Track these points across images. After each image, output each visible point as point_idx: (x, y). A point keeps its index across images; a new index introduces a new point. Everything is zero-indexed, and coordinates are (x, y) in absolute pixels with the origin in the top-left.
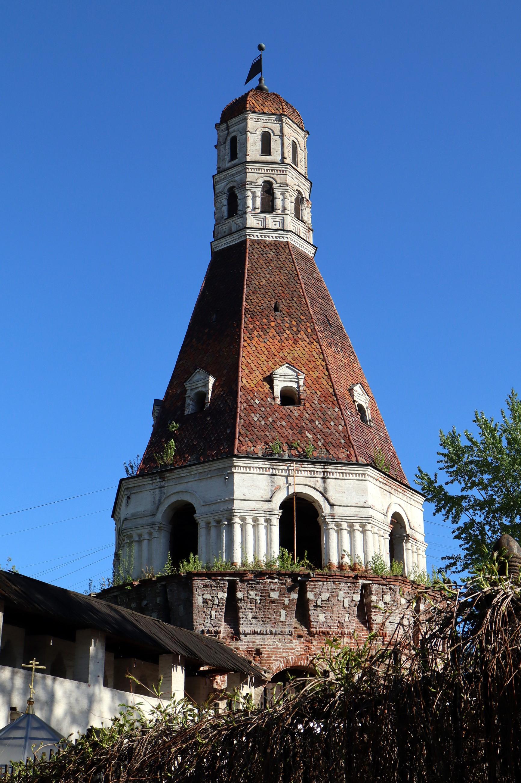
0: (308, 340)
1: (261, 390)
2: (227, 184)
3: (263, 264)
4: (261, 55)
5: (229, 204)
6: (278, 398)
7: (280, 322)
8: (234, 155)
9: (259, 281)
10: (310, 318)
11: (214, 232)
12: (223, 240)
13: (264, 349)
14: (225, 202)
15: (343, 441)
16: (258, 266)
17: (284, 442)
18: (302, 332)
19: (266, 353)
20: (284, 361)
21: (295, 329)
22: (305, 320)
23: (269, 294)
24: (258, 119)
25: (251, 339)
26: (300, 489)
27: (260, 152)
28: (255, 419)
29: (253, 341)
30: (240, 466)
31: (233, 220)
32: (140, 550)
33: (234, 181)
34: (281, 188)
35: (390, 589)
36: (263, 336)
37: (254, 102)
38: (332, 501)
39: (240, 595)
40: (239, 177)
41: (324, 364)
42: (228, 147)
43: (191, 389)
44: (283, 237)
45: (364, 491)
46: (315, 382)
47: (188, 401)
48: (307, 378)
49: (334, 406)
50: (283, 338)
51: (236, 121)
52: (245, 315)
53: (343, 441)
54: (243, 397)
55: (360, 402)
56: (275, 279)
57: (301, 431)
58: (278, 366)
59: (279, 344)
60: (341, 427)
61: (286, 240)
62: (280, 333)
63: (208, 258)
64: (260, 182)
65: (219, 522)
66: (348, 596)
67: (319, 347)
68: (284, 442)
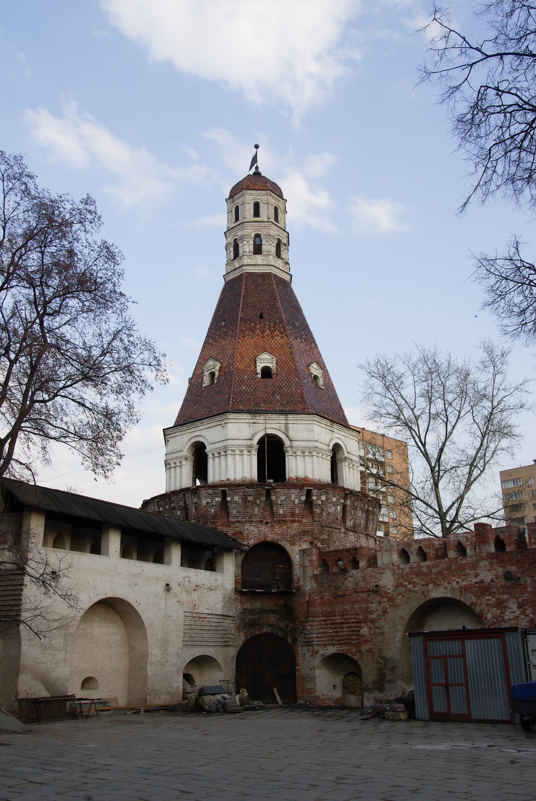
0: (281, 336)
1: (248, 369)
8: (237, 219)
10: (282, 321)
13: (251, 343)
14: (232, 249)
15: (300, 400)
17: (261, 402)
18: (277, 331)
19: (253, 345)
21: (272, 329)
25: (244, 337)
26: (269, 431)
27: (253, 215)
28: (244, 388)
29: (245, 339)
32: (175, 473)
35: (325, 492)
36: (251, 335)
38: (291, 438)
39: (229, 499)
41: (290, 350)
42: (234, 213)
45: (312, 431)
46: (284, 363)
47: (205, 378)
48: (279, 361)
49: (295, 377)
50: (264, 335)
53: (300, 400)
54: (237, 374)
55: (315, 374)
57: (273, 394)
59: (261, 339)
60: (299, 391)
61: (270, 271)
62: (263, 332)
64: (253, 235)
65: (219, 453)
66: (297, 497)
68: (261, 402)
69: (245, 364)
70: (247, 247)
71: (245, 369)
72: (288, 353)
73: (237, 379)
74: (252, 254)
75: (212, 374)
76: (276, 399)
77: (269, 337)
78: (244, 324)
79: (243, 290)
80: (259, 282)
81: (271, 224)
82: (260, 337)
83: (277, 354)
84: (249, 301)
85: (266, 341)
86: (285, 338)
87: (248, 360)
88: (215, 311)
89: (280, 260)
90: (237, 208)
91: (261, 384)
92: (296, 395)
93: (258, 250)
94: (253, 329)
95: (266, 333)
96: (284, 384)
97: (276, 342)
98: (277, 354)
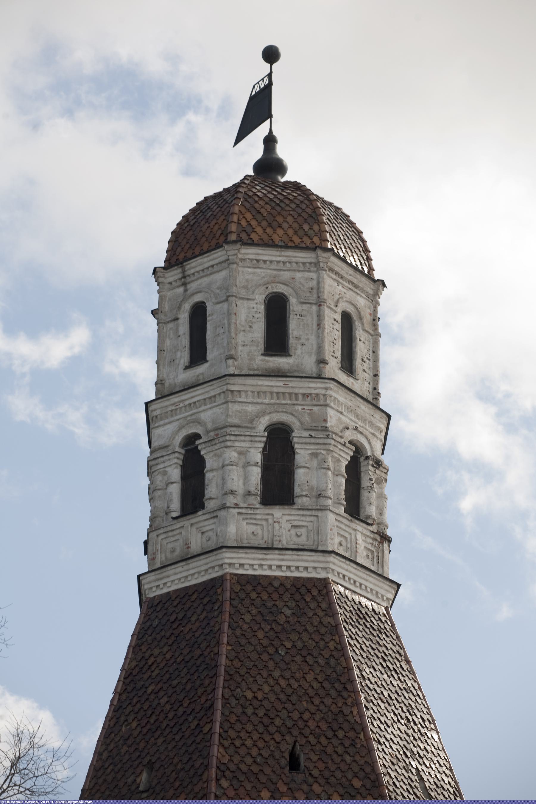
2: (181, 428)
3: (265, 642)
4: (270, 75)
5: (184, 477)
8: (198, 354)
9: (255, 687)
12: (170, 571)
14: (175, 474)
16: (251, 648)
22: (363, 790)
23: (278, 722)
24: (258, 261)
27: (261, 347)
31: (193, 521)
33: (198, 422)
34: (313, 440)
37: (248, 216)
40: (209, 413)
44: (315, 568)
51: (206, 265)
52: (218, 780)
56: (292, 681)
61: (322, 575)
70: (238, 470)
74: (255, 501)
79: (224, 649)
80: (282, 619)
81: (332, 385)
84: (249, 695)
88: (109, 719)
89: (360, 527)
90: (199, 313)
93: (278, 487)
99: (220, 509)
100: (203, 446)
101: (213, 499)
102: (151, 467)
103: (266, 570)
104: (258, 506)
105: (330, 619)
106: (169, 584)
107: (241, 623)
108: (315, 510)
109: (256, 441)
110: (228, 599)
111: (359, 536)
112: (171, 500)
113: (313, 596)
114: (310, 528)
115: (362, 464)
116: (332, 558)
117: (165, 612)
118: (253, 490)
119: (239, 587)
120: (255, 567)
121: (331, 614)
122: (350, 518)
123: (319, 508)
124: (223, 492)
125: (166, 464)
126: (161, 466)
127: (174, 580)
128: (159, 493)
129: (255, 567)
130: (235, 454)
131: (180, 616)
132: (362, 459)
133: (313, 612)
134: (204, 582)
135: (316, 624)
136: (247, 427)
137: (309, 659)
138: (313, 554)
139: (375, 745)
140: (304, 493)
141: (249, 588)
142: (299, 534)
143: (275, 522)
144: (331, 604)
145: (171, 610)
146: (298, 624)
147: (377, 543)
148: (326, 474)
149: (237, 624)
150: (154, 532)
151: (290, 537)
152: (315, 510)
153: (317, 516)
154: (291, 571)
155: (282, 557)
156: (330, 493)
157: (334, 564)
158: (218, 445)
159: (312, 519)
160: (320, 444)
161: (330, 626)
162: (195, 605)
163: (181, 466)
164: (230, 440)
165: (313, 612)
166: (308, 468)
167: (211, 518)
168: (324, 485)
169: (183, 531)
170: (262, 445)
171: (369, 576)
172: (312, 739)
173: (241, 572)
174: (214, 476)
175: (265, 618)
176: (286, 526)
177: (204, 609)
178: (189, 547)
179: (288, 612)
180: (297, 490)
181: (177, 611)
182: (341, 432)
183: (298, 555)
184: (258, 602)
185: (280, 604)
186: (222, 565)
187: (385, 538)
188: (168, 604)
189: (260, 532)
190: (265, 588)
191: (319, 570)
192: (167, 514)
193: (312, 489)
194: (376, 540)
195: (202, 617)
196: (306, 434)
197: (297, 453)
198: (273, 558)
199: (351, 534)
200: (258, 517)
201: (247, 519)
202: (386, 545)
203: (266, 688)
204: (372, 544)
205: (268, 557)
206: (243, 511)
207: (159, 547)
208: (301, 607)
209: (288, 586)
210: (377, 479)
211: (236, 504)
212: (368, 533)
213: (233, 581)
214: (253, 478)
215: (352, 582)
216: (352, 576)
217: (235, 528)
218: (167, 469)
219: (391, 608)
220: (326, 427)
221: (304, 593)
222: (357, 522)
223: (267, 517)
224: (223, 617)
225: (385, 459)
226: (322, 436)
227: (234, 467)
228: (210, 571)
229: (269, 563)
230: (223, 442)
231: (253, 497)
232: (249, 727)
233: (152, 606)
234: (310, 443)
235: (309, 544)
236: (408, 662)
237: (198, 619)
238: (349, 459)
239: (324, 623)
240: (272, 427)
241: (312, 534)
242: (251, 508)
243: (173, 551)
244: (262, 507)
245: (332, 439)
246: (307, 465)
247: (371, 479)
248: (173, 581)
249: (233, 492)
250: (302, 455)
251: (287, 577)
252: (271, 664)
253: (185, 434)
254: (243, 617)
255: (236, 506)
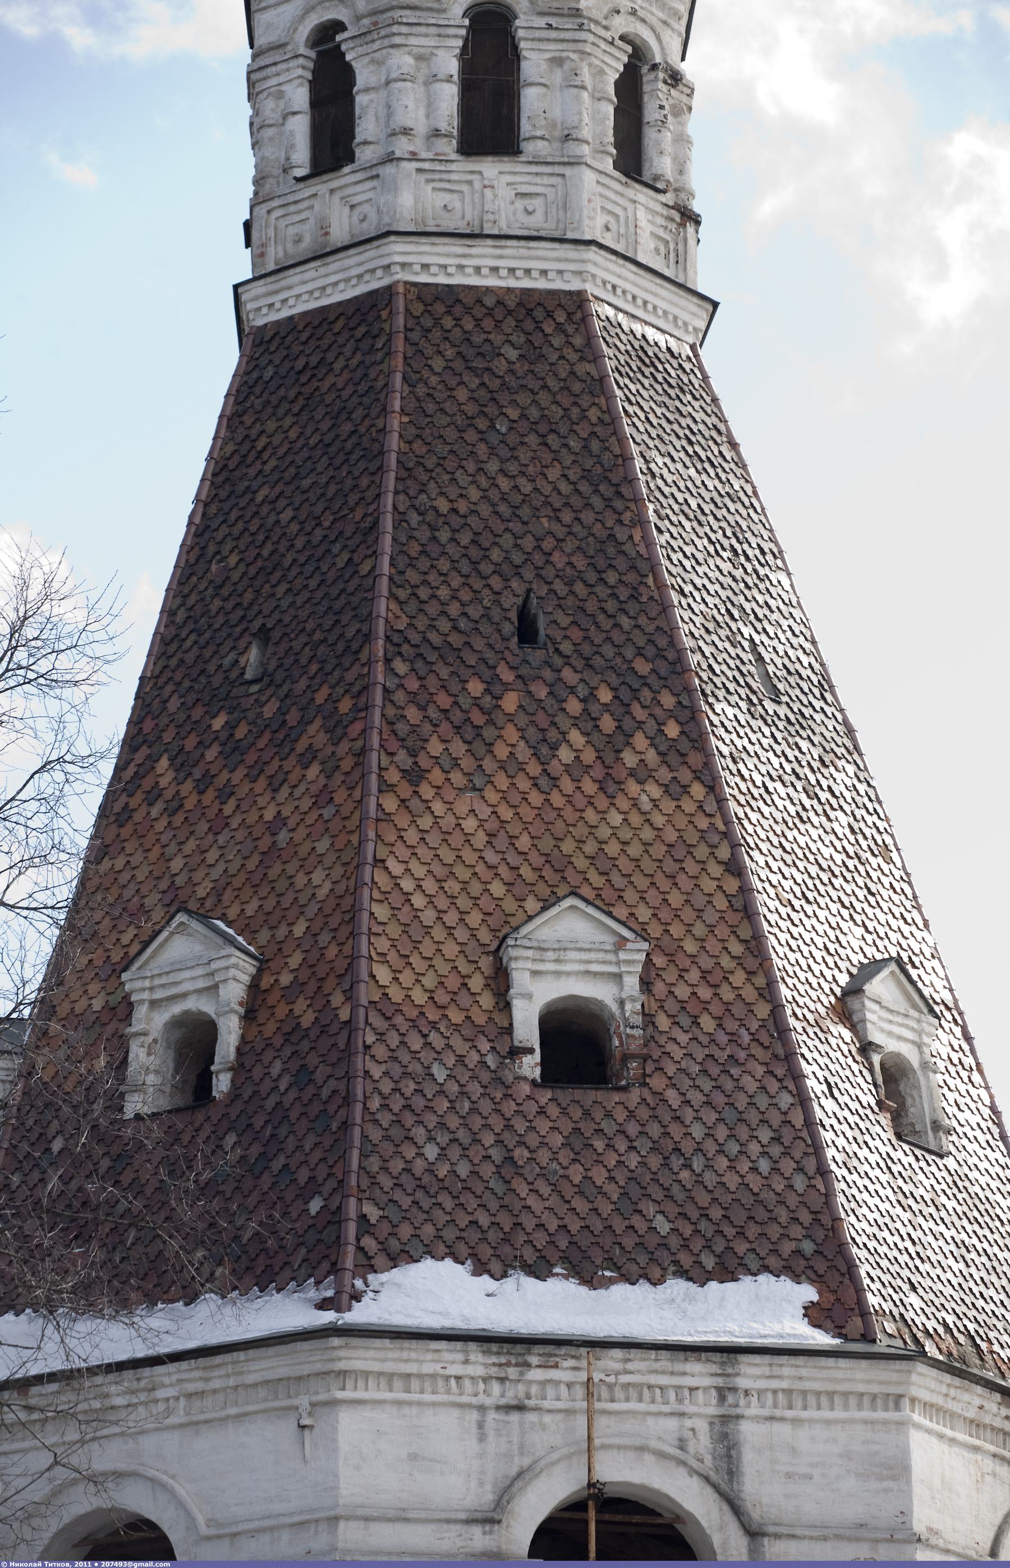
0: (664, 774)
3: (471, 409)
5: (315, 104)
6: (531, 1051)
7: (542, 692)
9: (453, 492)
11: (247, 226)
12: (293, 277)
13: (470, 824)
14: (300, 96)
16: (445, 420)
18: (640, 741)
19: (480, 839)
20: (555, 882)
21: (607, 723)
22: (653, 680)
23: (496, 555)
25: (415, 776)
26: (618, 1471)
29: (427, 792)
30: (366, 1374)
34: (553, 34)
36: (467, 763)
41: (732, 885)
43: (154, 1004)
44: (560, 272)
45: (897, 1470)
47: (138, 1054)
50: (555, 767)
52: (388, 661)
53: (808, 1247)
55: (891, 1045)
56: (522, 481)
57: (629, 1204)
58: (532, 905)
59: (536, 798)
61: (575, 285)
62: (545, 746)
63: (224, 358)
67: (711, 807)
69: (429, 981)
70: (414, 88)
71: (433, 1015)
72: (721, 903)
73: (386, 1086)
74: (449, 147)
75: (195, 1039)
76: (652, 1241)
77: (589, 787)
78: (413, 685)
79: (395, 423)
80: (500, 366)
82: (523, 784)
83: (644, 914)
84: (443, 505)
85: (569, 814)
86: (698, 790)
87: (450, 949)
89: (642, 195)
91: (543, 1126)
92: (783, 1216)
93: (490, 122)
94: (478, 718)
95: (565, 755)
96: (698, 1131)
97: (635, 819)
98: (644, 914)
99: (383, 163)
100: (351, 44)
101: (370, 143)
102: (254, 83)
103: (470, 275)
104: (454, 156)
105: (589, 367)
106: (291, 302)
107: (425, 373)
108: (559, 163)
109: (448, 36)
110: (402, 329)
111: (641, 214)
112: (293, 146)
113: (558, 324)
114: (550, 197)
115: (645, 79)
116: (592, 254)
117: (285, 353)
118: (443, 126)
119: (421, 308)
120: (450, 270)
121: (591, 358)
122: (624, 179)
123: (566, 160)
124: (389, 131)
125: (282, 79)
126: (273, 82)
127: (300, 295)
128: (269, 132)
129: (450, 270)
130: (410, 60)
131: (314, 360)
132: (645, 69)
133: (558, 353)
134: (356, 297)
135: (563, 375)
136: (431, 9)
137: (552, 440)
138: (557, 245)
139: (675, 596)
140: (539, 133)
141: (439, 308)
142: (530, 209)
143: (485, 187)
144: (590, 339)
145: (296, 349)
146: (530, 376)
147: (674, 226)
148: (578, 98)
149: (418, 376)
150: (263, 206)
151: (514, 214)
152: (559, 163)
153: (563, 175)
154: (517, 278)
155: (498, 252)
156: (586, 133)
157: (595, 264)
158: (378, 43)
159: (554, 180)
160: (568, 41)
161: (589, 379)
162: (341, 340)
163: (310, 82)
164: (400, 34)
165: (558, 353)
166: (545, 85)
167: (367, 179)
168: (576, 118)
169: (316, 203)
170: (460, 43)
171: (661, 286)
172: (559, 586)
173: (423, 278)
174: (372, 101)
175: (470, 364)
176: (506, 193)
177: (357, 349)
178: (327, 234)
179: (513, 354)
180: (526, 128)
181: (308, 352)
182: (606, 18)
183: (529, 248)
184: (457, 334)
185: (497, 339)
186: (389, 266)
187: (689, 217)
188: (290, 338)
189: (458, 205)
190: (468, 310)
191: (567, 276)
192: (285, 171)
193: (554, 125)
194: (673, 220)
195: (355, 361)
196: (541, 22)
197: (525, 58)
198: (483, 254)
199: (625, 209)
200: (454, 177)
201: (433, 181)
202: (690, 229)
203: (474, 494)
204: (666, 228)
205: (473, 251)
206: (426, 166)
207: (271, 233)
208: (536, 344)
209: (511, 304)
210: (673, 107)
211: (414, 154)
212: (659, 208)
213: (409, 297)
214: (444, 105)
215: (629, 297)
216: (628, 286)
217: (411, 197)
218: (283, 88)
219: (701, 345)
220: (578, 10)
221: (541, 319)
222: (637, 186)
223: (470, 177)
224: (393, 363)
225: (686, 68)
226: (570, 26)
227: (408, 84)
228: (367, 277)
229: (476, 262)
230: (386, 36)
231: (445, 140)
232: (444, 565)
233: (261, 343)
234: (548, 40)
235: (549, 228)
236: (734, 445)
237: (347, 366)
238: (622, 69)
239: (579, 374)
240: (477, 9)
241: (554, 210)
242: (441, 161)
243: (298, 240)
244: (461, 158)
245: (590, 31)
246: (543, 81)
247: (662, 107)
248: (298, 296)
249: (406, 131)
250: (534, 62)
251: (509, 289)
252: (482, 450)
253: (316, 22)
254: (430, 362)
255: (414, 157)
